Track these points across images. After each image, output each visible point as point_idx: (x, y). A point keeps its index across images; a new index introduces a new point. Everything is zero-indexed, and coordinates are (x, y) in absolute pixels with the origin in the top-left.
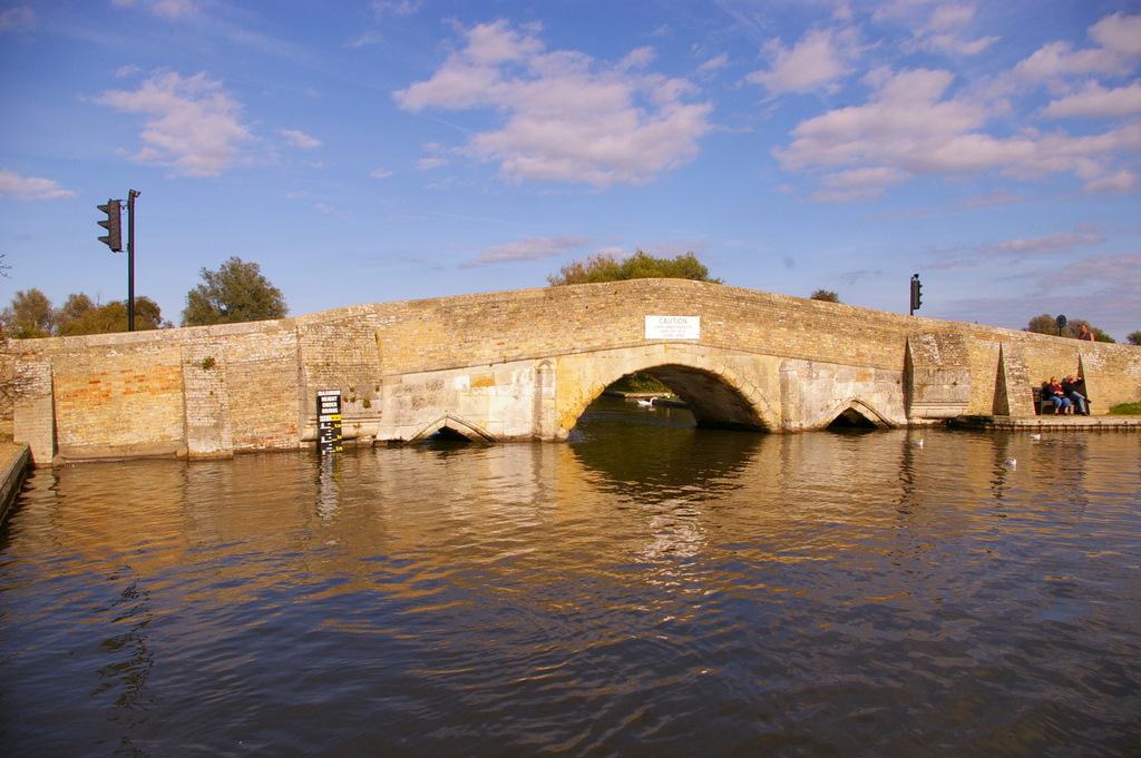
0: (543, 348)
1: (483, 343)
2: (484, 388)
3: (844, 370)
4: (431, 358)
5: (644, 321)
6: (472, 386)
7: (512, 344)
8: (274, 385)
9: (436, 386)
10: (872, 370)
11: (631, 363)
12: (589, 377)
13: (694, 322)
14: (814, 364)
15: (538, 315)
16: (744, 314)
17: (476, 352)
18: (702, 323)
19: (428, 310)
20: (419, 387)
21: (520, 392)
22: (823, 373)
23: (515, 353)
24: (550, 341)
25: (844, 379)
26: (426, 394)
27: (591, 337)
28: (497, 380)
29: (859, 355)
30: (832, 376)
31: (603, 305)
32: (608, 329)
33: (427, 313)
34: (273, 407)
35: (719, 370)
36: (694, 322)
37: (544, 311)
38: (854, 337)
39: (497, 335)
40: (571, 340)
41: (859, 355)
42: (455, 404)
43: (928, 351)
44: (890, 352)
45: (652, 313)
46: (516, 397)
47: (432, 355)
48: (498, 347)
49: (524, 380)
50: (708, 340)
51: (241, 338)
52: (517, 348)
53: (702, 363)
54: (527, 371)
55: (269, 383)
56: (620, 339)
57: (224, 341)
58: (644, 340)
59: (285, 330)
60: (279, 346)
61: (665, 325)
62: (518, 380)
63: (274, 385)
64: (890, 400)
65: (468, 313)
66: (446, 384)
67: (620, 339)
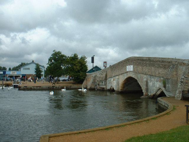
11: (125, 77)
12: (122, 79)
13: (132, 66)
16: (139, 64)
18: (133, 67)
22: (153, 79)
25: (157, 81)
29: (159, 73)
30: (154, 80)
35: (136, 78)
36: (132, 66)
38: (158, 67)
41: (159, 73)
44: (166, 72)
45: (127, 65)
50: (134, 71)
53: (133, 76)
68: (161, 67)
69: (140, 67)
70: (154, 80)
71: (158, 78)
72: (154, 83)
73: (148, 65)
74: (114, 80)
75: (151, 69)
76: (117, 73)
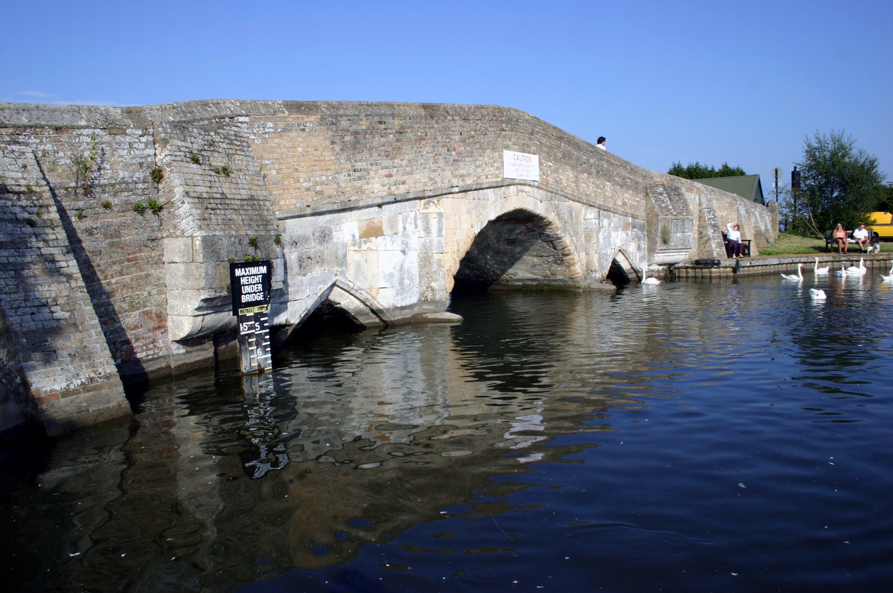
0: (425, 184)
1: (372, 173)
2: (373, 239)
3: (616, 219)
4: (320, 193)
5: (501, 156)
6: (360, 237)
7: (400, 178)
8: (128, 237)
9: (324, 236)
10: (630, 219)
14: (601, 212)
15: (422, 139)
17: (365, 187)
18: (541, 163)
19: (312, 118)
20: (306, 239)
21: (407, 244)
23: (402, 189)
24: (433, 175)
25: (616, 229)
26: (313, 248)
27: (464, 172)
28: (386, 229)
29: (624, 204)
31: (473, 133)
32: (478, 163)
33: (311, 120)
34: (127, 278)
37: (426, 135)
38: (622, 186)
39: (387, 162)
40: (448, 174)
41: (624, 204)
42: (342, 262)
43: (663, 202)
45: (507, 147)
46: (404, 252)
47: (318, 188)
48: (386, 180)
49: (410, 228)
51: (64, 137)
52: (404, 183)
53: (539, 209)
54: (412, 215)
55: (117, 234)
56: (487, 178)
57: (33, 140)
58: (503, 179)
59: (136, 127)
60: (128, 159)
61: (518, 162)
62: (405, 228)
63: (128, 237)
64: (639, 248)
65: (354, 127)
66: (334, 233)
67: (487, 178)
68: (628, 188)
69: (570, 174)
70: (609, 225)
71: (620, 219)
72: (609, 234)
73: (593, 170)
74: (372, 232)
75: (602, 187)
76: (419, 180)
